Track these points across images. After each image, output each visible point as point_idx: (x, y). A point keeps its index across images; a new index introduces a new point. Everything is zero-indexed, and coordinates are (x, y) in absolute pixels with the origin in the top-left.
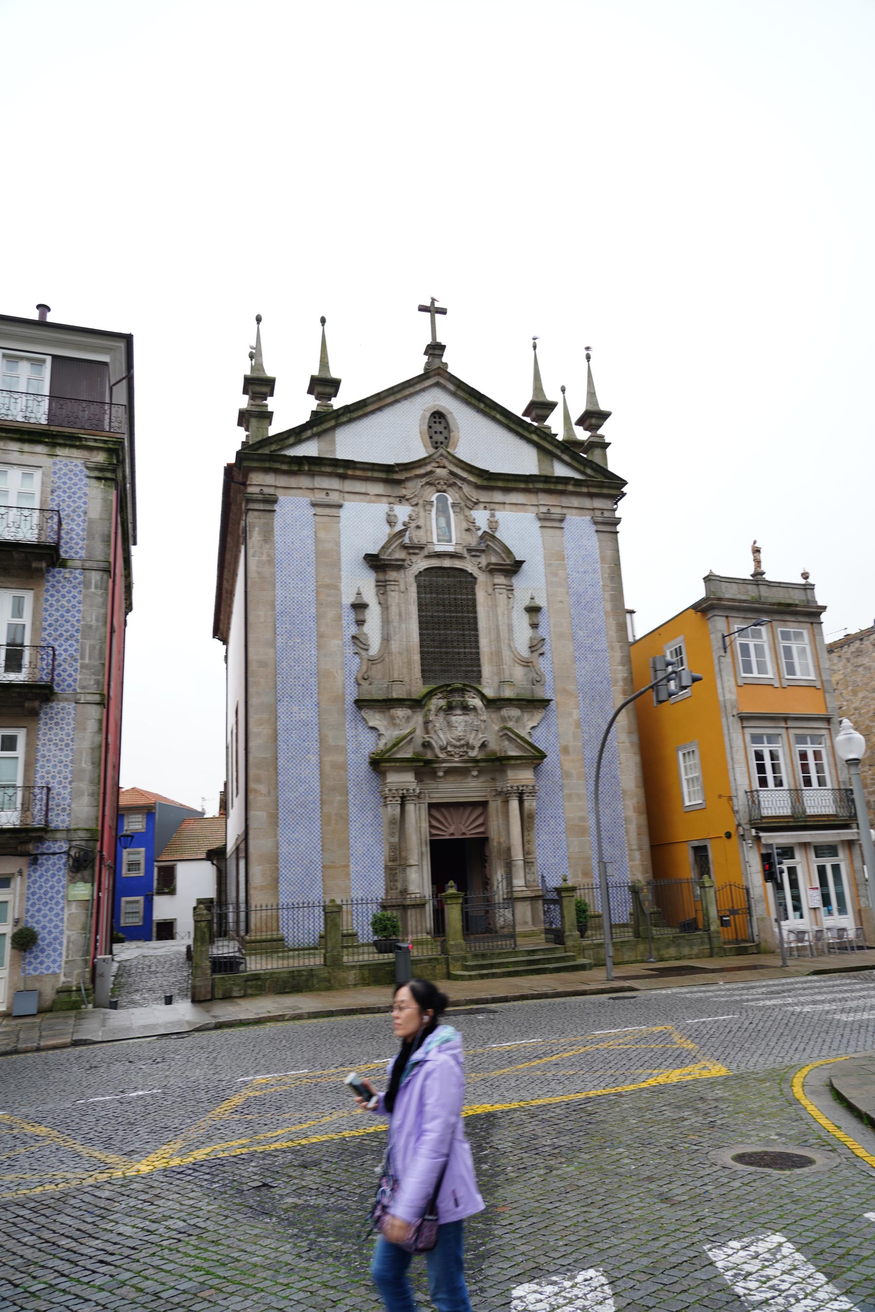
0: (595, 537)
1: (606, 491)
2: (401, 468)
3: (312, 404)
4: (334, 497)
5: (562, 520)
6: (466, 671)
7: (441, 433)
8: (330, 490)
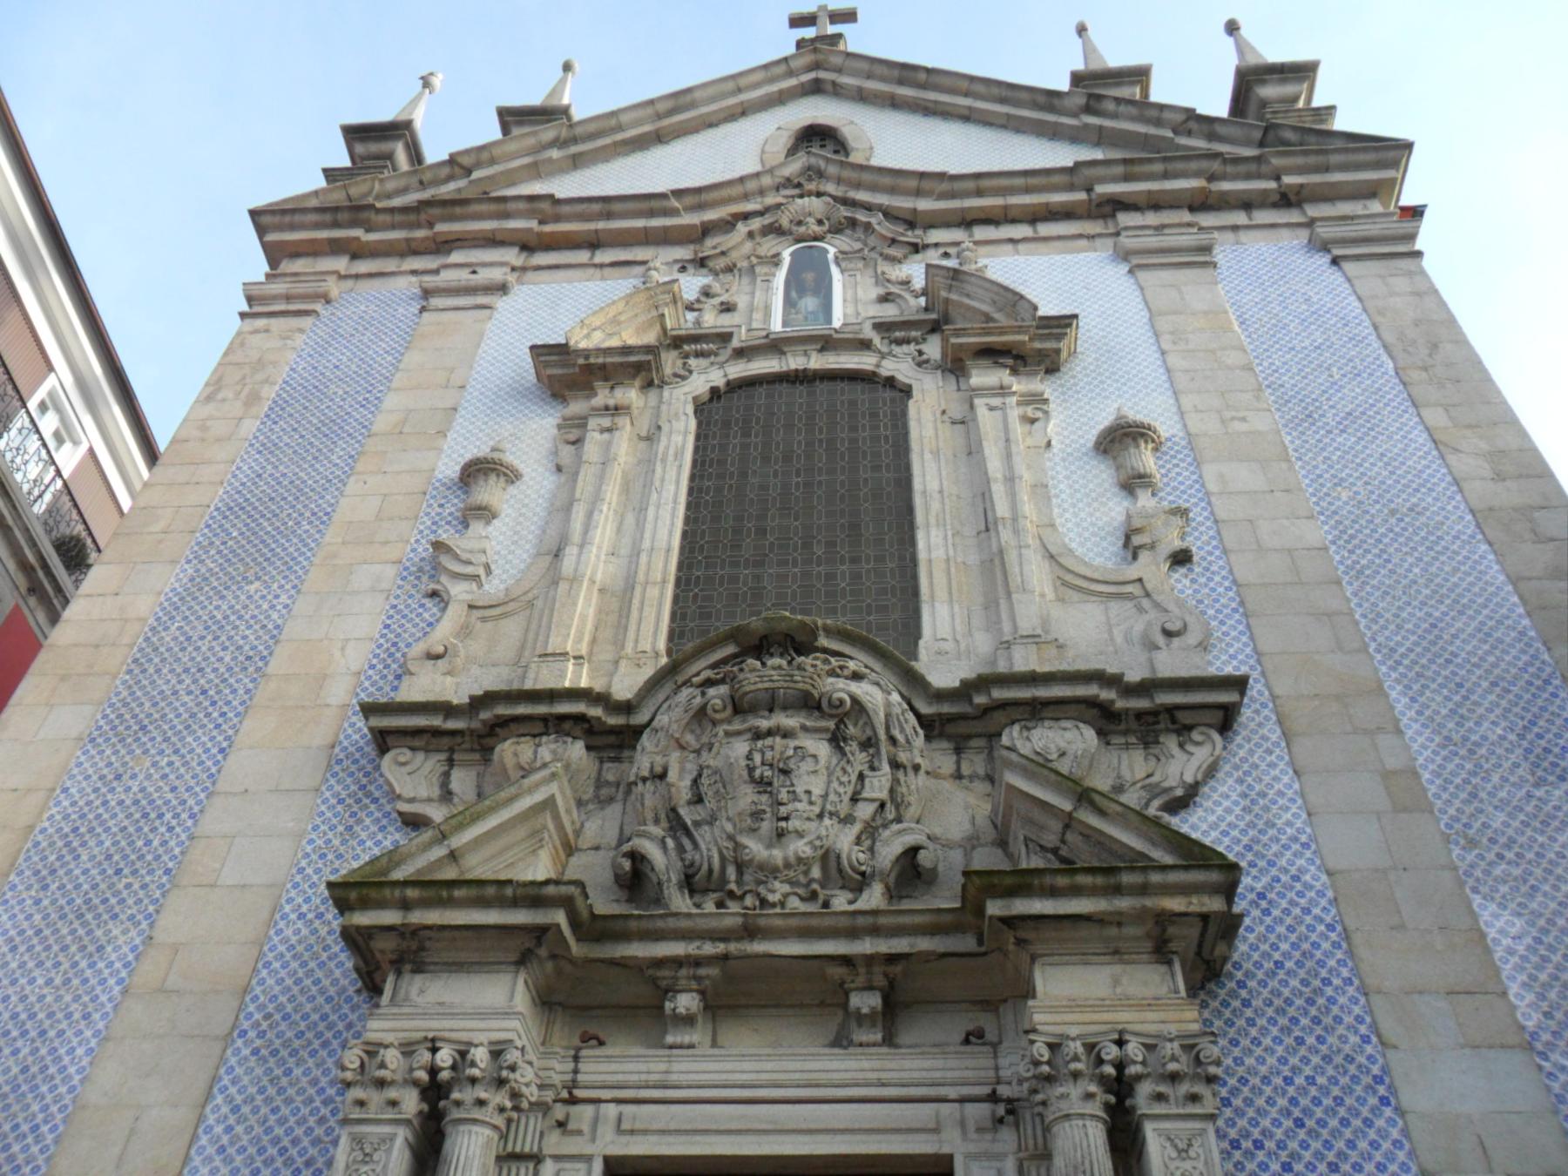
0: (1334, 277)
2: (689, 200)
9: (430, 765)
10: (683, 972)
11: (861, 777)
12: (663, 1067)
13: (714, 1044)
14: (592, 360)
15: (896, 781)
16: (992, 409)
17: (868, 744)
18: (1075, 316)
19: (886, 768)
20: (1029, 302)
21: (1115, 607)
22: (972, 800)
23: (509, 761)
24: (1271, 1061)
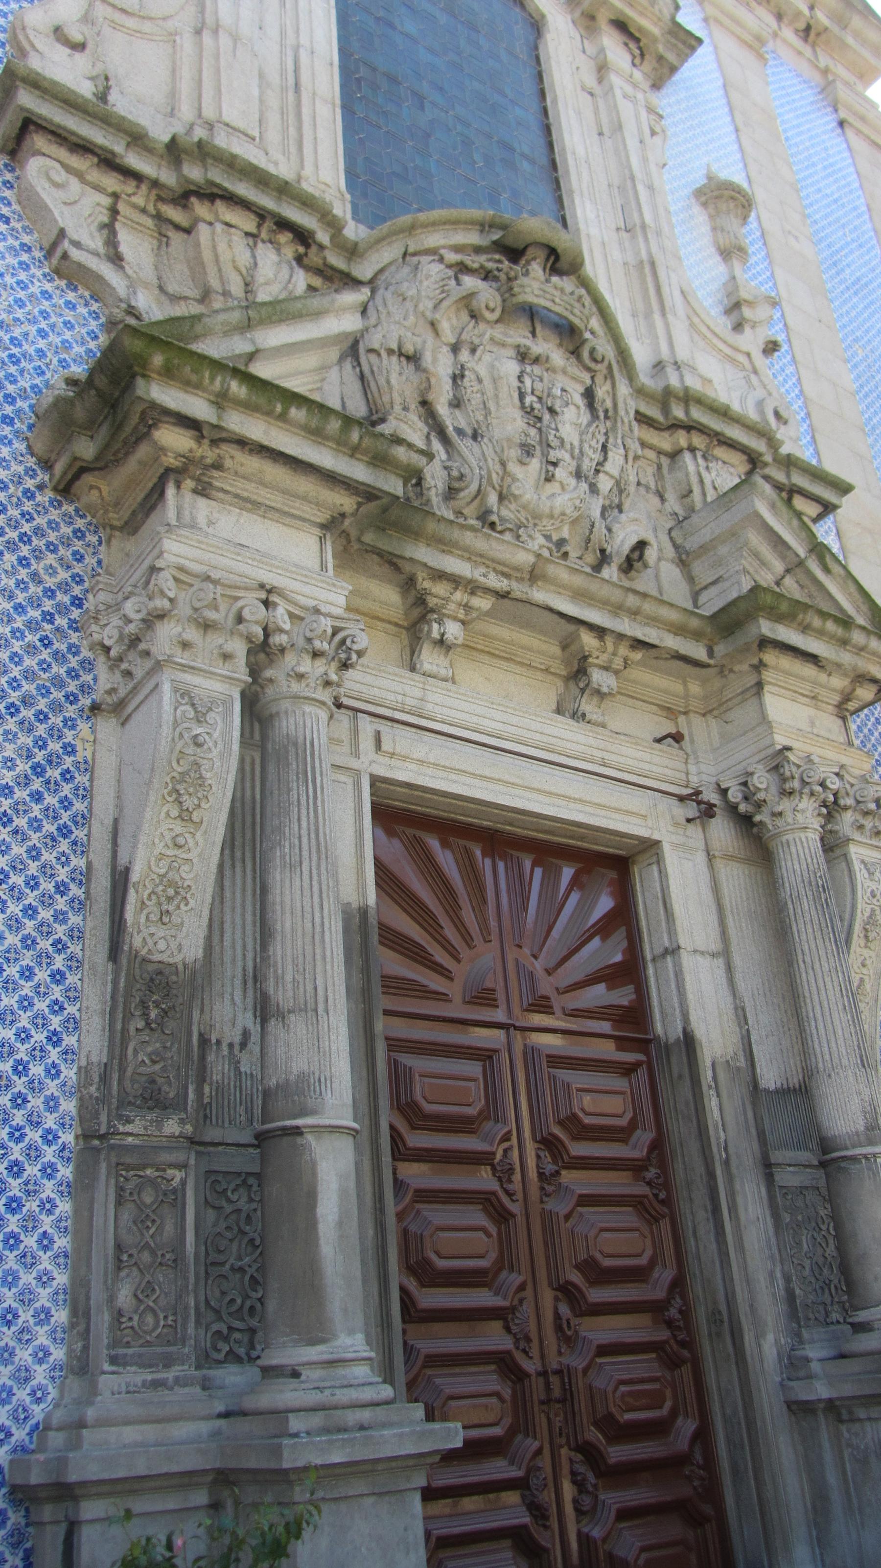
10: (458, 596)
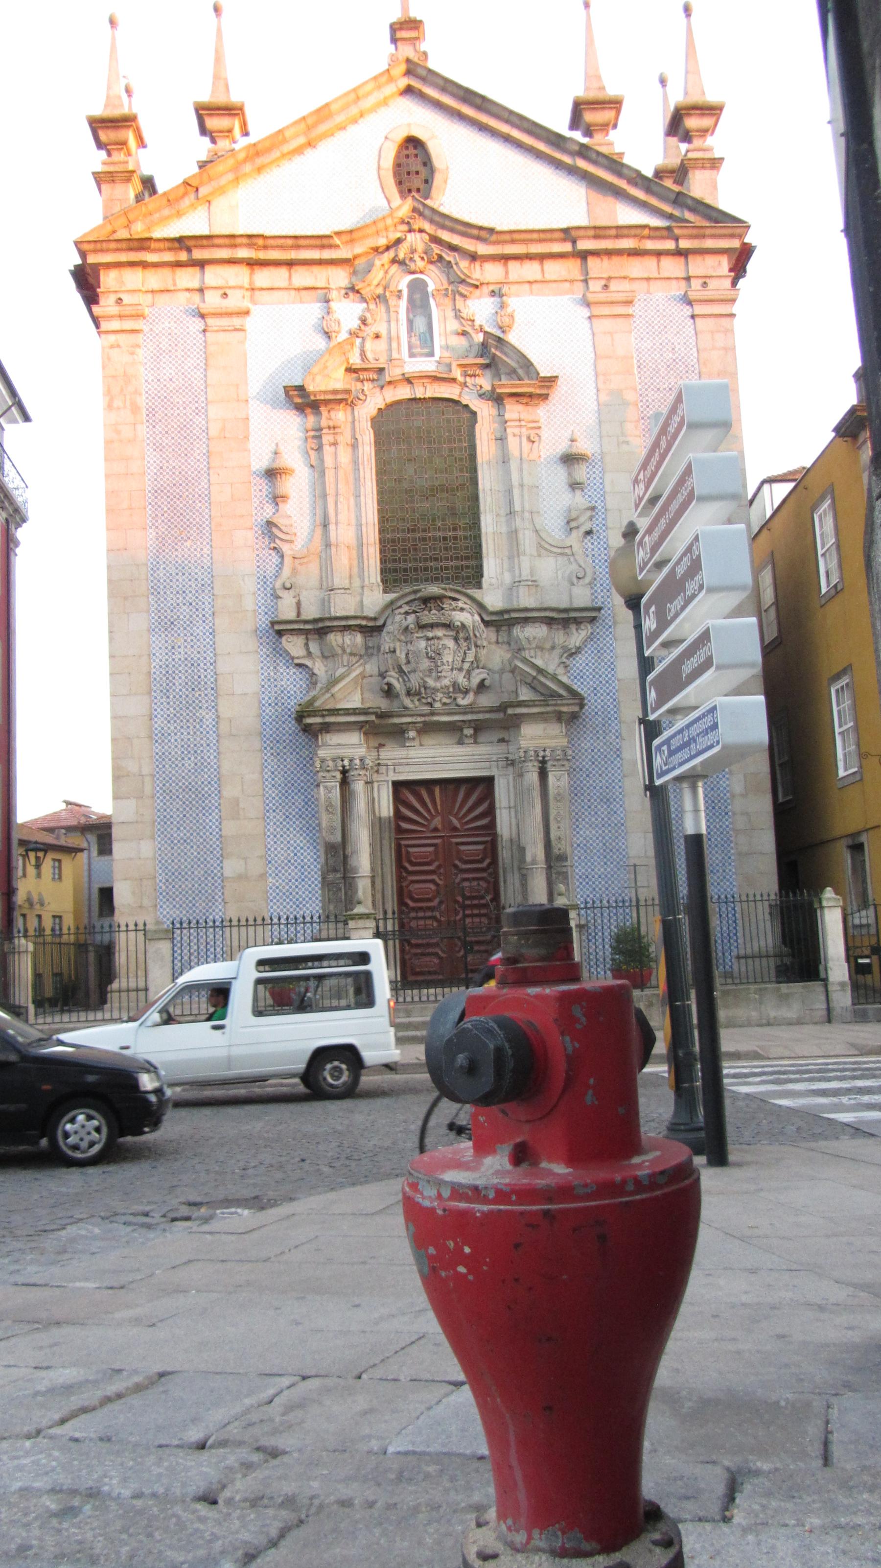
1: (709, 244)
2: (345, 238)
3: (203, 147)
4: (236, 301)
5: (629, 303)
6: (457, 568)
7: (417, 173)
8: (230, 288)
9: (299, 641)
11: (465, 653)
12: (405, 752)
13: (421, 745)
14: (318, 398)
15: (477, 652)
16: (514, 435)
17: (467, 639)
18: (557, 377)
19: (473, 649)
20: (536, 370)
21: (560, 558)
22: (502, 653)
23: (334, 644)
24: (589, 744)
